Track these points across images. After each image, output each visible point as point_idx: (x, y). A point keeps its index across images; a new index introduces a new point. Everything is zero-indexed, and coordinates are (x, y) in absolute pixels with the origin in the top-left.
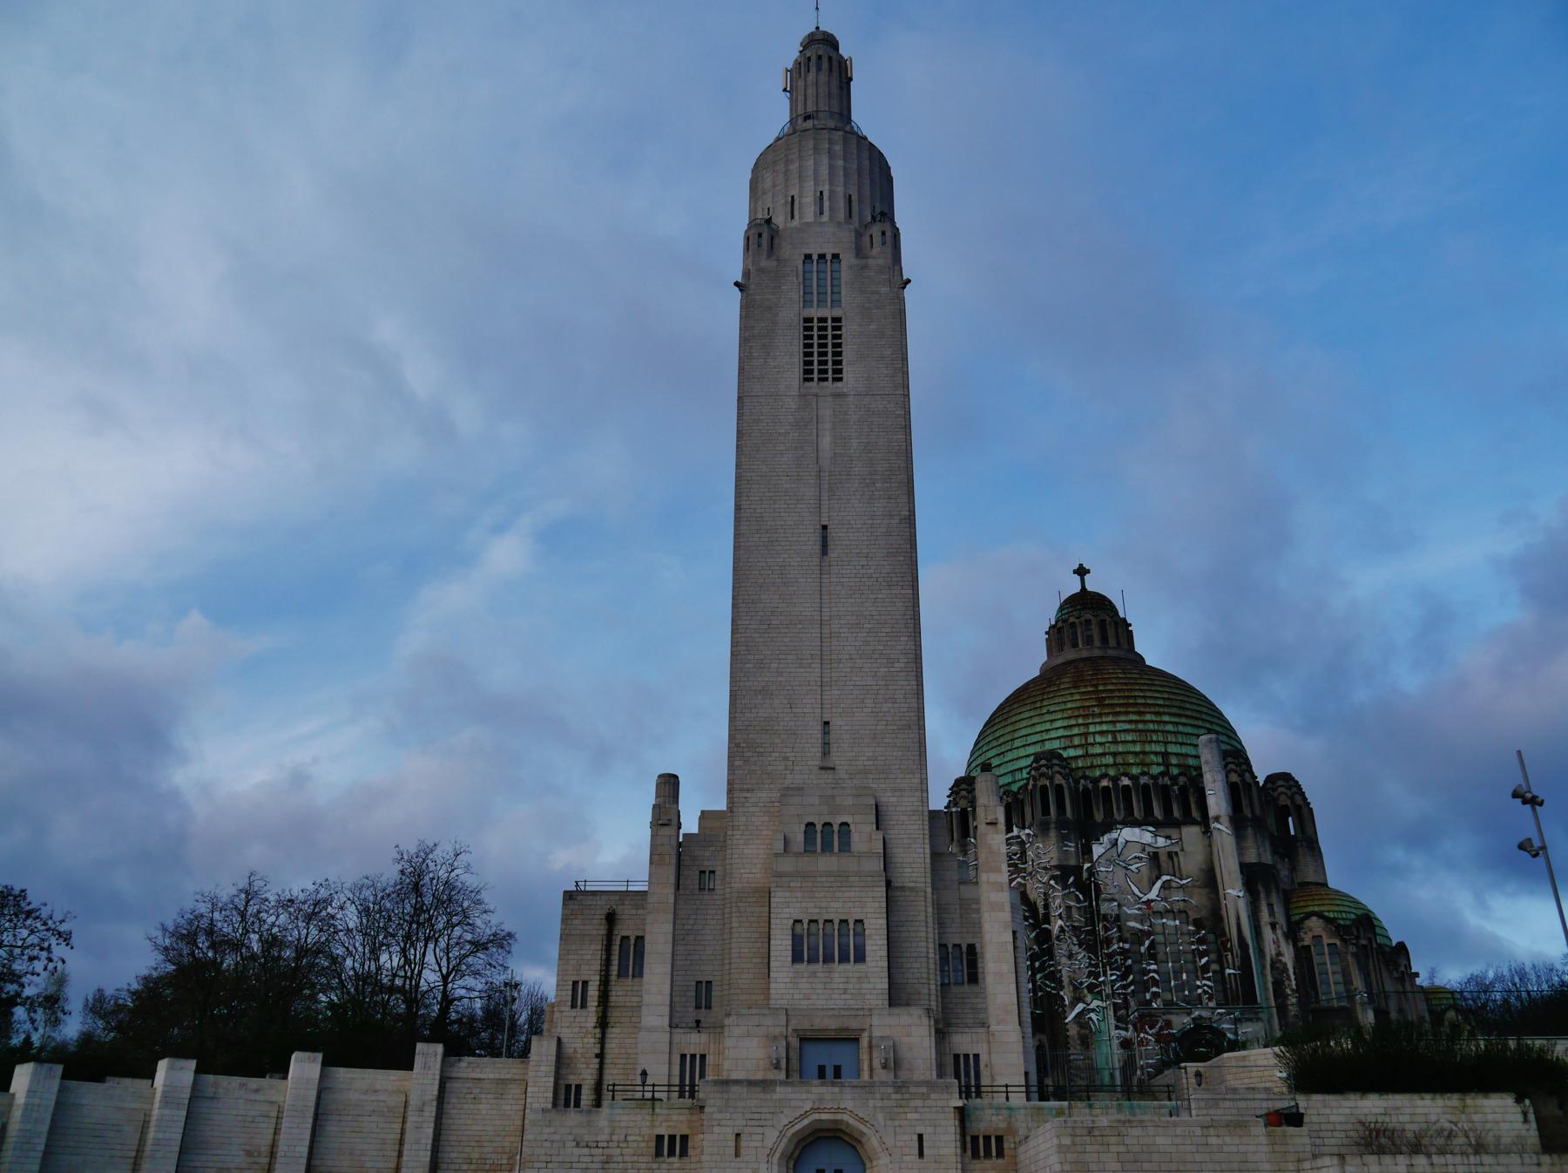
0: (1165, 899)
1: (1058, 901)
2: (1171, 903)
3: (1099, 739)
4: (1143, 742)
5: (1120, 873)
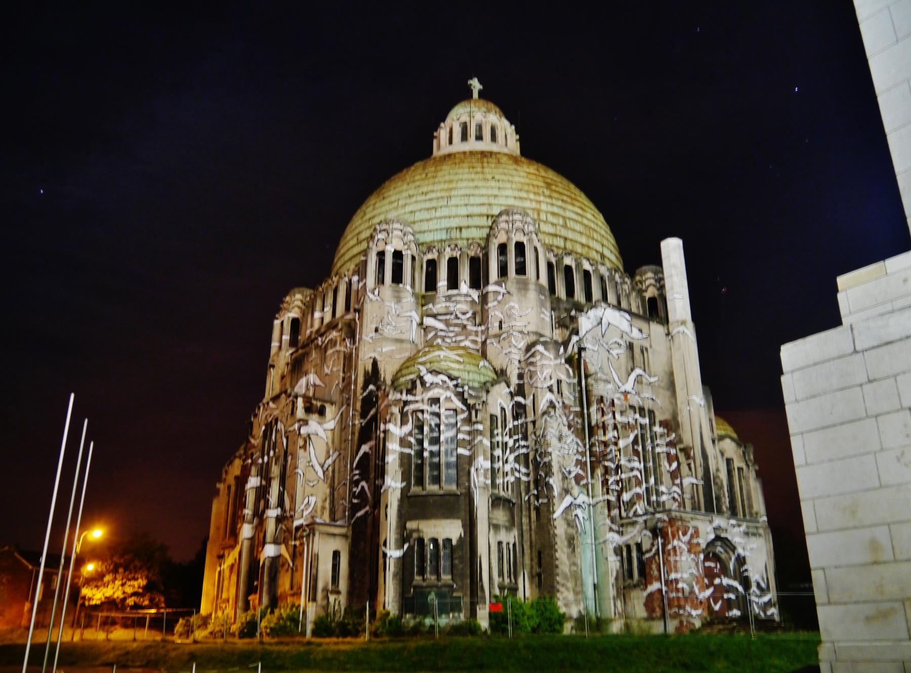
0: (638, 393)
1: (547, 372)
2: (643, 399)
4: (588, 237)
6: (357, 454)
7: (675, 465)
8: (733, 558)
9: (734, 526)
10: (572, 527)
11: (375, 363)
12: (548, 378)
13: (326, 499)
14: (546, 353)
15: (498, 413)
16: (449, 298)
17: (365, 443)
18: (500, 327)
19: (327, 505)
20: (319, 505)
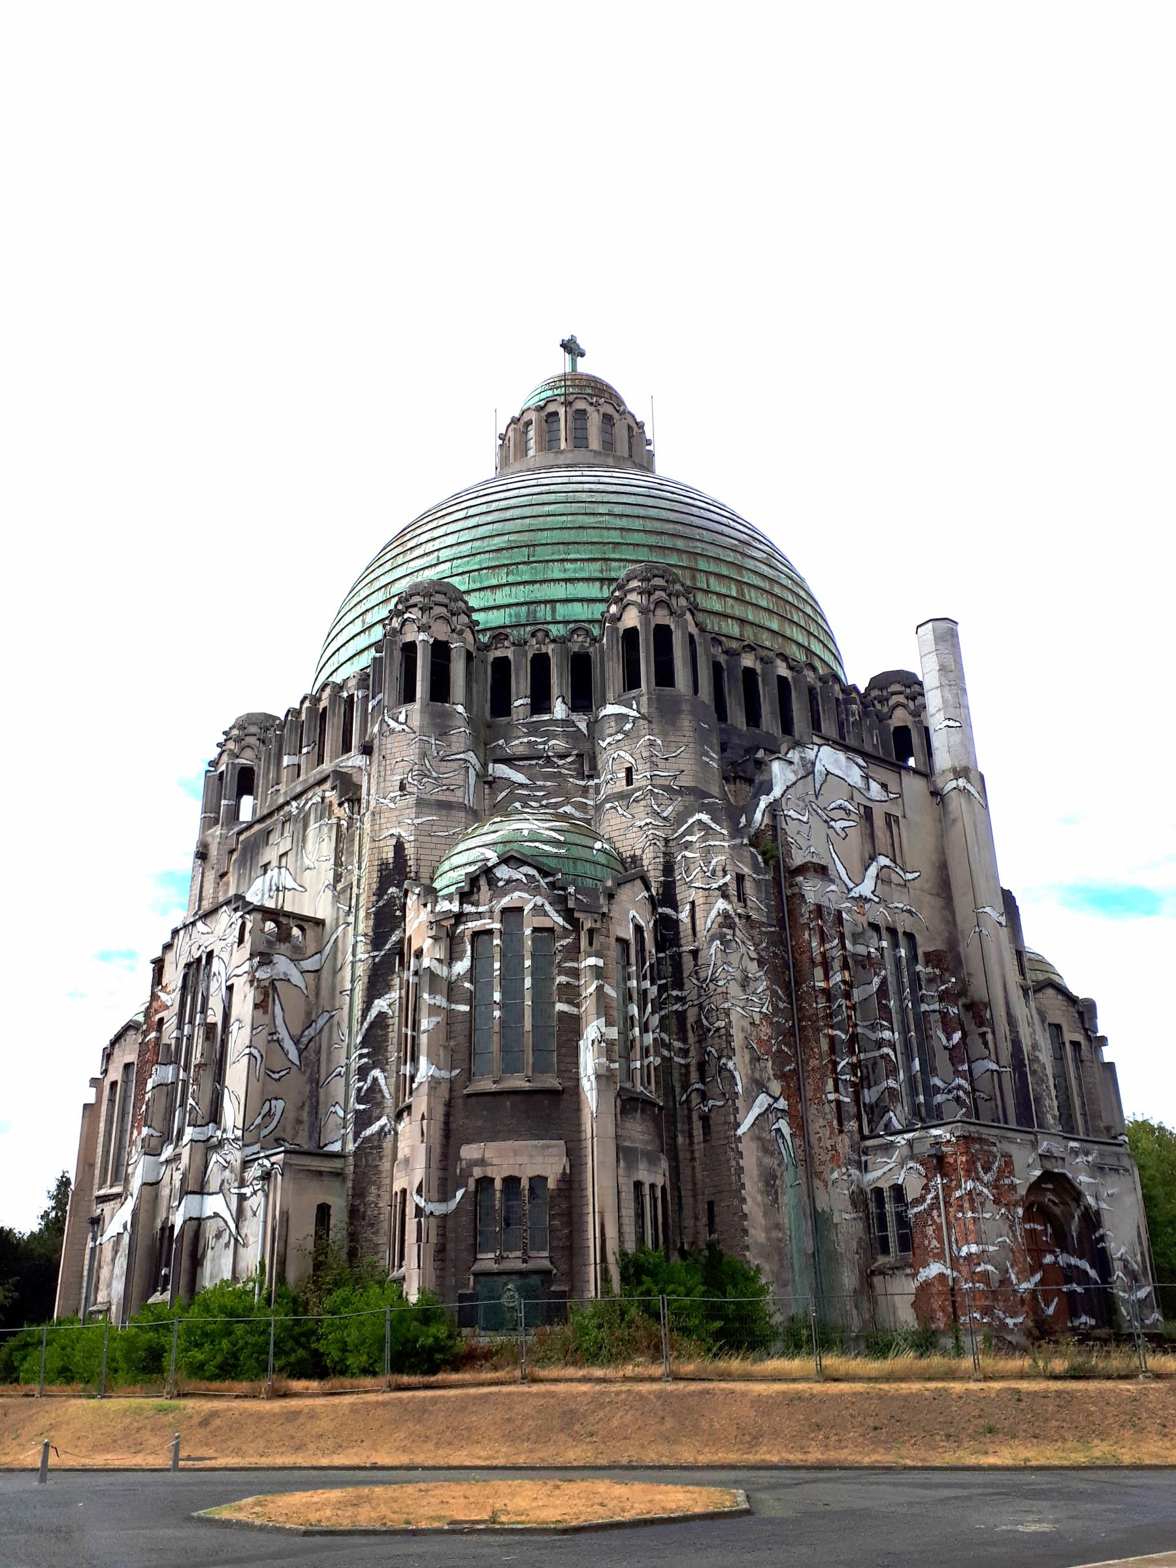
3: (715, 585)
5: (819, 828)
6: (364, 1016)
7: (957, 1036)
8: (1077, 1215)
9: (1075, 1153)
10: (772, 1154)
11: (399, 847)
12: (721, 874)
13: (303, 1105)
14: (713, 825)
15: (629, 934)
16: (534, 729)
17: (380, 996)
18: (629, 781)
19: (305, 1116)
20: (291, 1115)
